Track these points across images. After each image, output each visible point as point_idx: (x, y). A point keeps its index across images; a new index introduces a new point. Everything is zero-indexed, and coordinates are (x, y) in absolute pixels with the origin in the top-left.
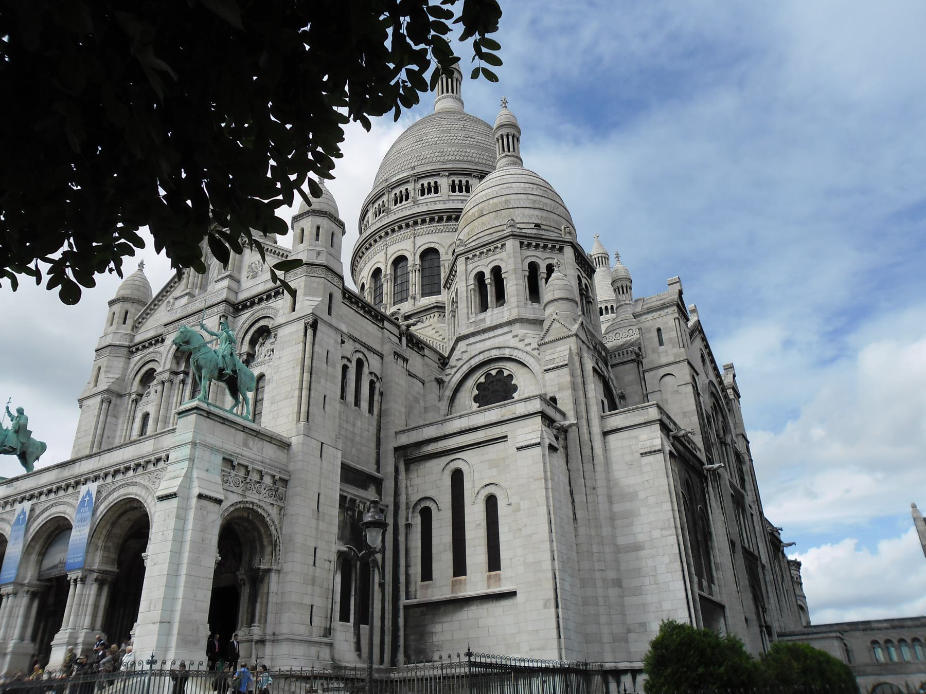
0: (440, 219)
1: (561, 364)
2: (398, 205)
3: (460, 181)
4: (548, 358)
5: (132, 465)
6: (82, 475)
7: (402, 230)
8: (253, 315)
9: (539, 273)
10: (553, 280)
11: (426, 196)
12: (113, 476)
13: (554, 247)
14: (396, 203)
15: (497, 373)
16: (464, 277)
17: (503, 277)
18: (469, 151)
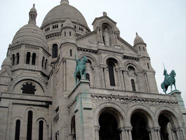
5: (166, 102)
6: (148, 99)
8: (128, 61)
12: (159, 102)
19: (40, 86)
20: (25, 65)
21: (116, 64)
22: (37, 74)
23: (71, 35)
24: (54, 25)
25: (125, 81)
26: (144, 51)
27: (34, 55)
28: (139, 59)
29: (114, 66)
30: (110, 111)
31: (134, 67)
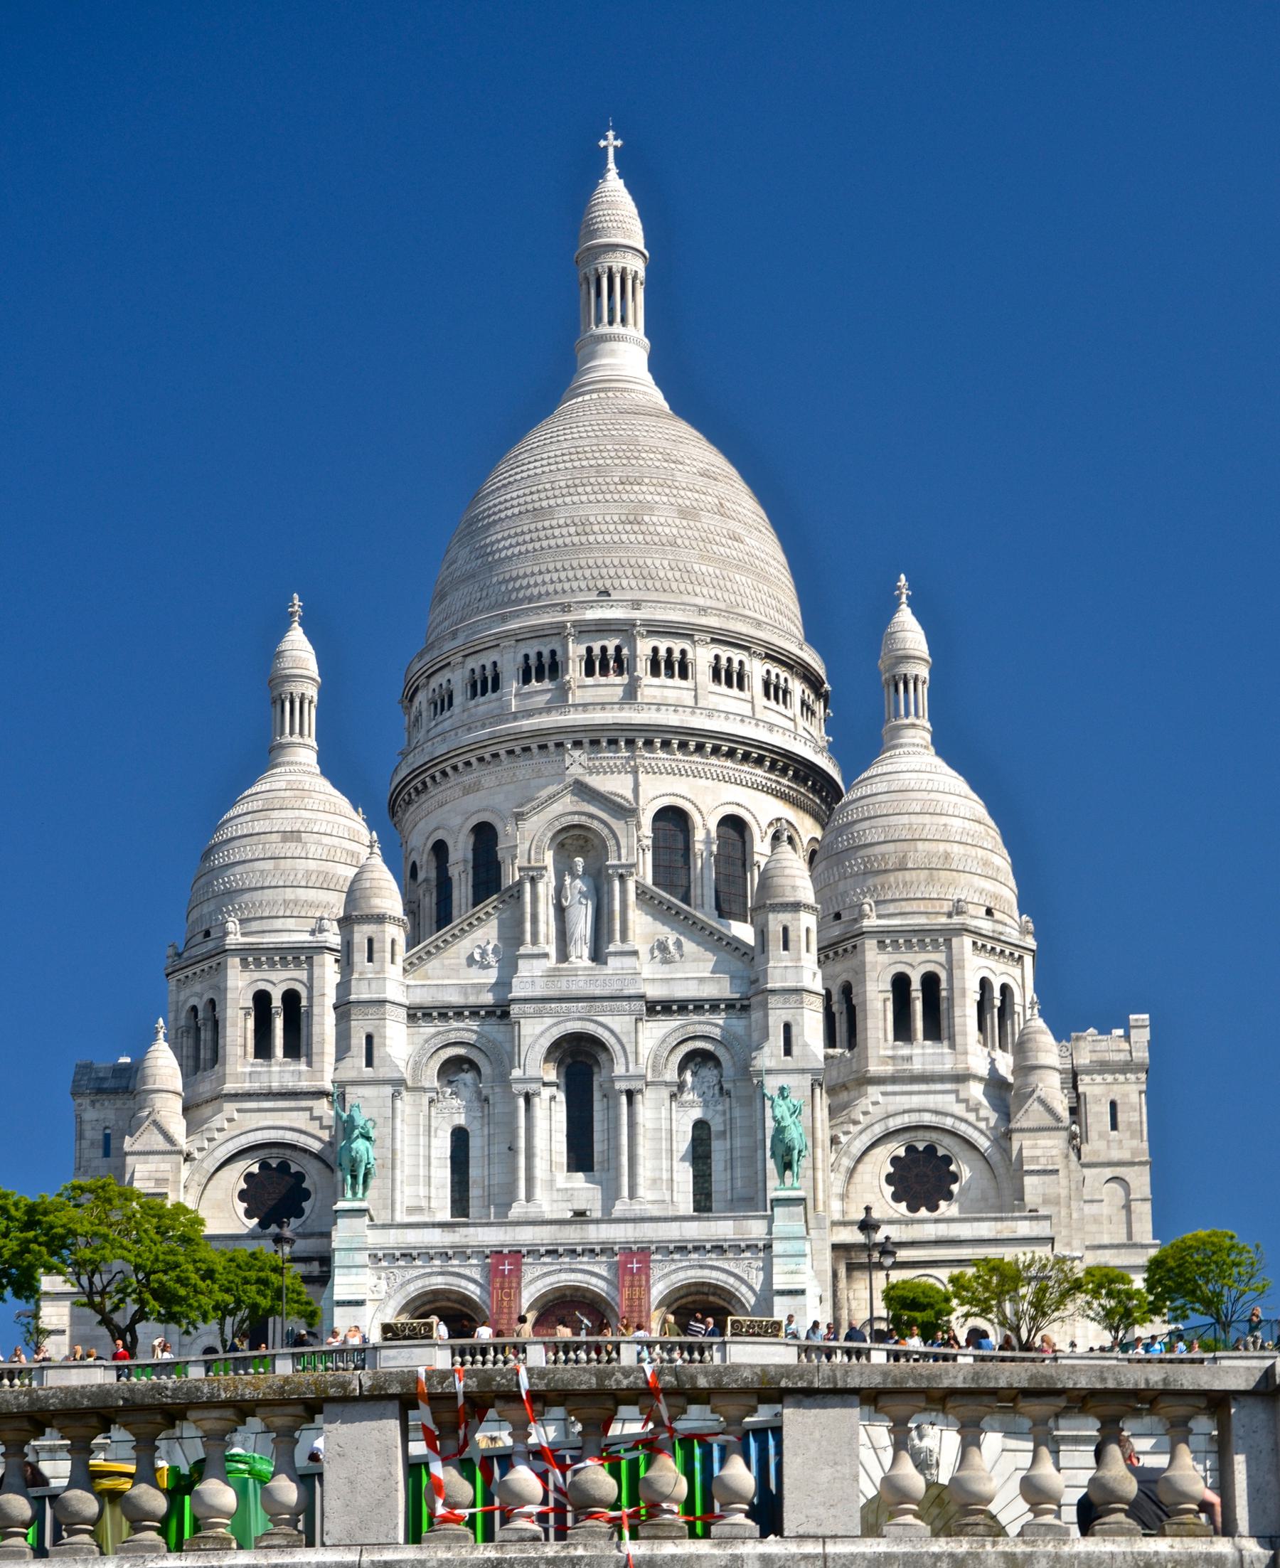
0: (700, 748)
1: (1050, 1167)
2: (598, 679)
3: (729, 660)
4: (1025, 1153)
5: (708, 1246)
6: (615, 1243)
7: (613, 747)
8: (683, 1026)
9: (987, 995)
10: (1035, 1032)
11: (663, 680)
13: (1011, 954)
14: (590, 672)
15: (926, 1148)
16: (875, 975)
17: (944, 994)
18: (737, 577)
19: (328, 1170)
20: (248, 1069)
21: (602, 1057)
22: (310, 1109)
23: (376, 956)
24: (473, 663)
25: (641, 1140)
26: (786, 947)
27: (291, 998)
28: (753, 1000)
29: (596, 1070)
30: (449, 1300)
31: (721, 1053)
